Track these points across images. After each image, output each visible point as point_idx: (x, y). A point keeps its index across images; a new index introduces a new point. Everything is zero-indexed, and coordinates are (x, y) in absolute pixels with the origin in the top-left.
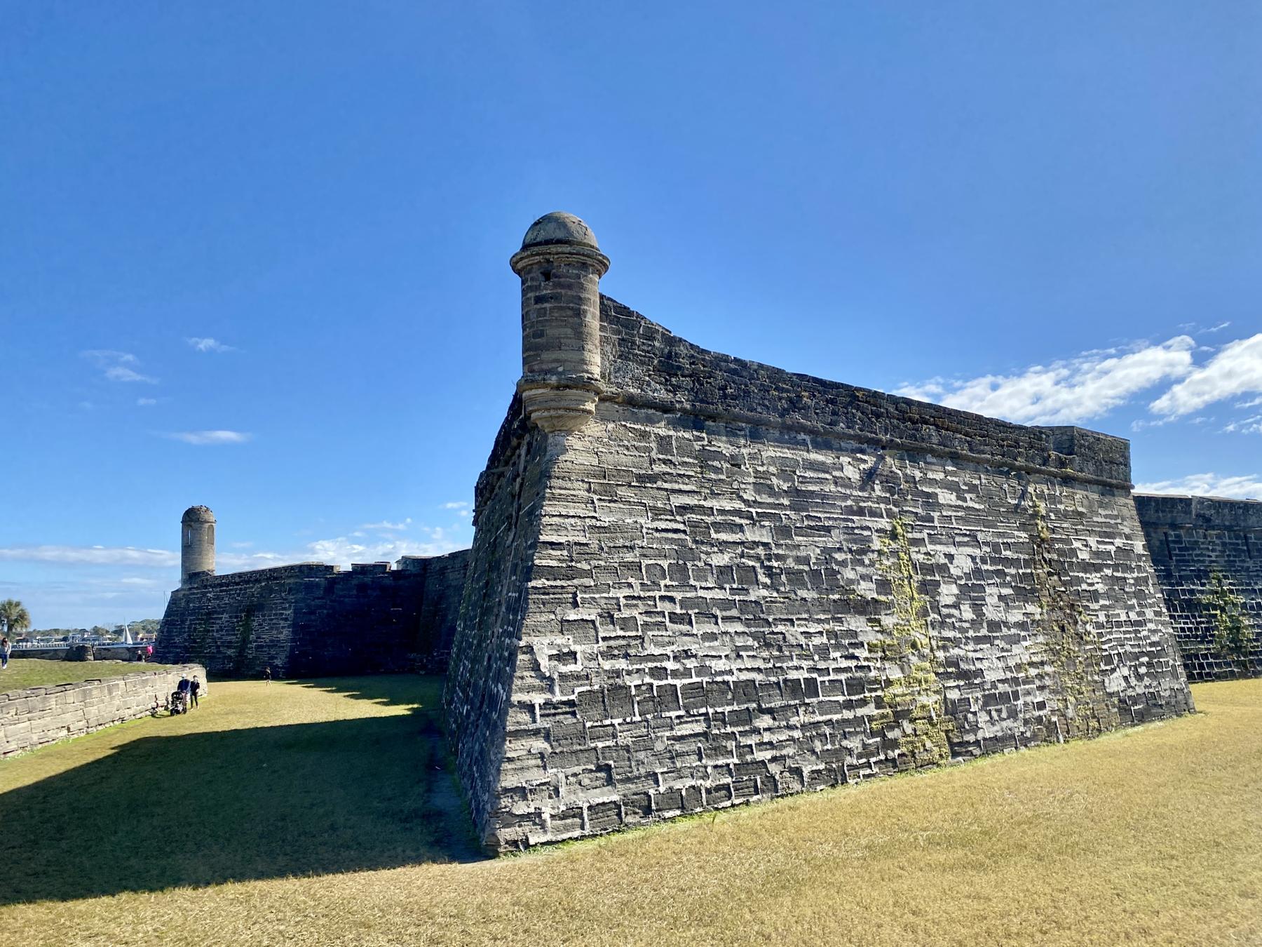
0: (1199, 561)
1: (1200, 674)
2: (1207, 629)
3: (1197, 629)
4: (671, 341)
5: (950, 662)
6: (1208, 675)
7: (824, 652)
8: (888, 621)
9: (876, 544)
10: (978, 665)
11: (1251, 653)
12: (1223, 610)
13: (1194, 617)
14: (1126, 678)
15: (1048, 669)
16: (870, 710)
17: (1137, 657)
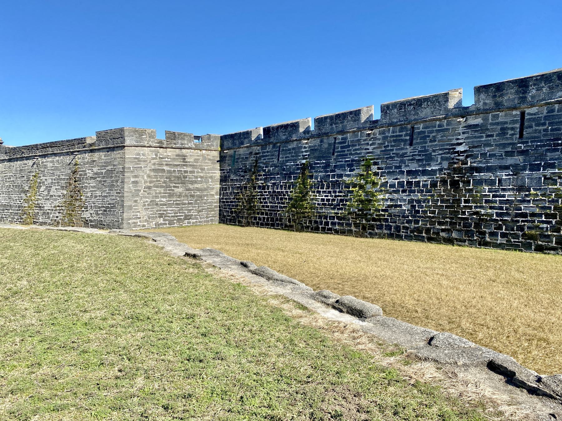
0: (356, 154)
1: (323, 229)
2: (342, 201)
3: (333, 200)
4: (5, 148)
5: (38, 204)
6: (330, 229)
7: (16, 200)
8: (28, 195)
9: (31, 179)
10: (45, 205)
11: (374, 220)
12: (361, 187)
13: (335, 192)
14: (91, 214)
15: (63, 208)
16: (20, 212)
17: (99, 208)
